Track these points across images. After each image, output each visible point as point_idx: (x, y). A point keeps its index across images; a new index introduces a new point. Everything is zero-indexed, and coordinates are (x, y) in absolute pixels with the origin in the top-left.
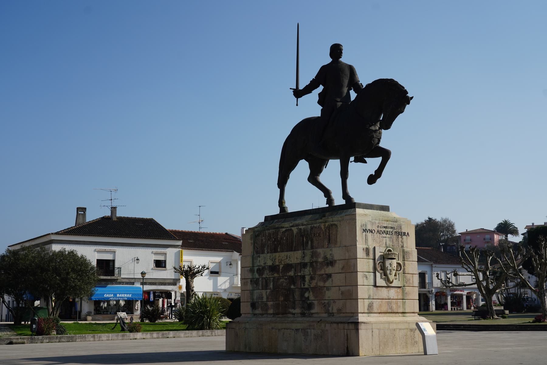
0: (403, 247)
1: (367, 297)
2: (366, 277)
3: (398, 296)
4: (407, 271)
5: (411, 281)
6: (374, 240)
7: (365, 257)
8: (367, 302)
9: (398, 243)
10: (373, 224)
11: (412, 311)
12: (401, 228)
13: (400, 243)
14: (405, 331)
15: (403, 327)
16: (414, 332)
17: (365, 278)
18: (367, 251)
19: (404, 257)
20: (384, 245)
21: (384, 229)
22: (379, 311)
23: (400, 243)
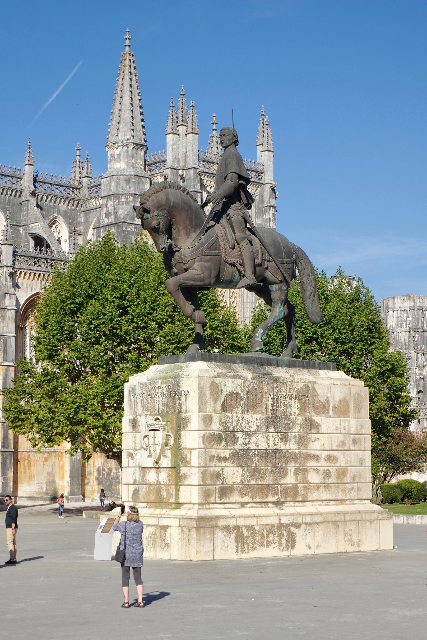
0: (180, 412)
1: (132, 482)
2: (132, 457)
3: (169, 480)
4: (183, 445)
5: (188, 460)
6: (143, 407)
7: (132, 431)
8: (132, 488)
9: (175, 407)
10: (143, 385)
11: (189, 502)
12: (178, 386)
13: (177, 406)
14: (153, 528)
15: (150, 524)
16: (165, 531)
17: (130, 458)
18: (134, 423)
19: (179, 427)
20: (156, 412)
21: (157, 390)
22: (146, 500)
23: (177, 406)
